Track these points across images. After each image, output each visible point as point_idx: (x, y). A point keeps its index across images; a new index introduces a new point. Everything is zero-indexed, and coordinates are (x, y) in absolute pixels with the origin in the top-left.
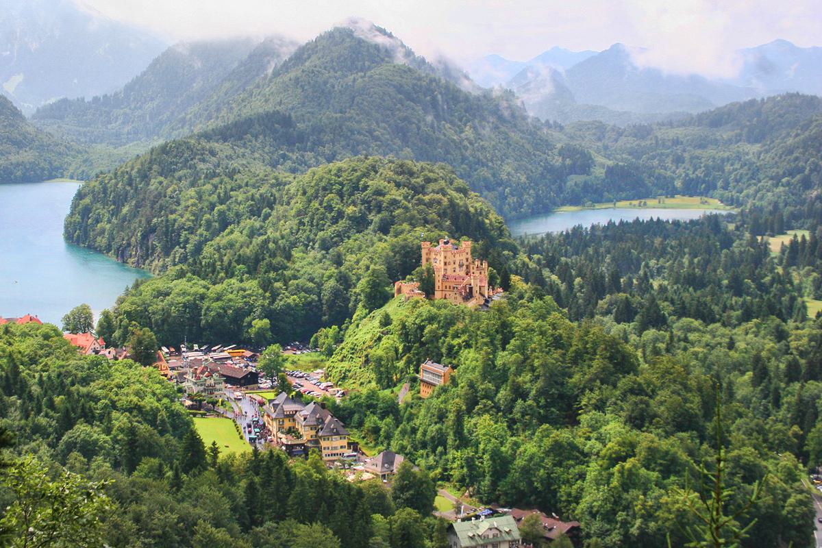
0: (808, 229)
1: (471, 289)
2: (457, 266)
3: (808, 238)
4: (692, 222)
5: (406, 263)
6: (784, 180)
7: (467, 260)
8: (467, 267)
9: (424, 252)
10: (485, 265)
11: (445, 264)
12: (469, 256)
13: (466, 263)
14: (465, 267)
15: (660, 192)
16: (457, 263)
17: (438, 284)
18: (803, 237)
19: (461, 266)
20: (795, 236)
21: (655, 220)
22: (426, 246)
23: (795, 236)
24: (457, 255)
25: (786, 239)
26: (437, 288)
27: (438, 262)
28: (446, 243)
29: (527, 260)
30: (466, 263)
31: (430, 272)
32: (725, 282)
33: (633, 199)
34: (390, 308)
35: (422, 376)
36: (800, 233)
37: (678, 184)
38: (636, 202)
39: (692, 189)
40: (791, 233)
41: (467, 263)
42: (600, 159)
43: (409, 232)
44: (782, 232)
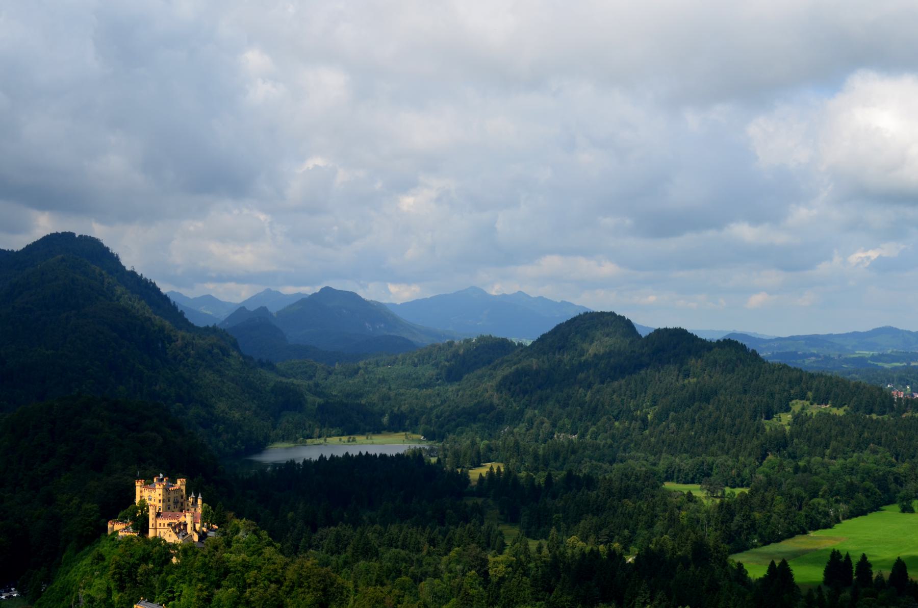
0: (502, 462)
1: (185, 525)
3: (502, 470)
4: (398, 455)
5: (122, 503)
6: (480, 416)
9: (138, 489)
15: (368, 428)
16: (172, 500)
18: (499, 469)
20: (491, 468)
21: (364, 453)
22: (138, 485)
23: (491, 468)
24: (172, 493)
25: (484, 471)
26: (150, 526)
28: (162, 480)
32: (429, 513)
33: (342, 435)
34: (104, 547)
36: (495, 466)
37: (385, 420)
38: (345, 438)
39: (398, 424)
40: (489, 465)
42: (310, 398)
44: (477, 465)
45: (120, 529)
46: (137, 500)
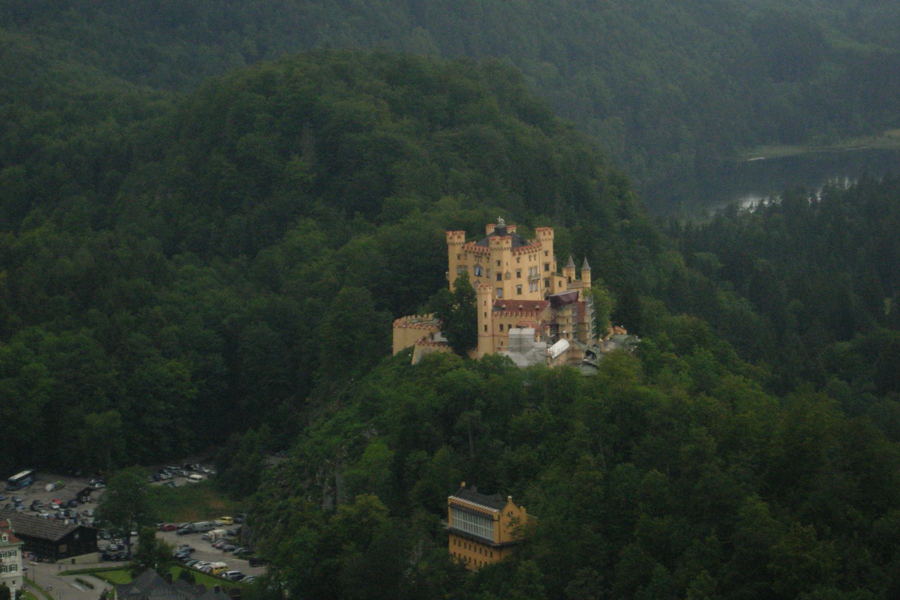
2: (524, 281)
7: (547, 267)
8: (547, 283)
9: (454, 252)
10: (587, 277)
11: (499, 277)
12: (551, 259)
13: (543, 274)
14: (542, 283)
16: (525, 274)
17: (482, 321)
19: (532, 281)
22: (456, 240)
26: (481, 330)
27: (484, 273)
29: (678, 260)
30: (543, 274)
31: (467, 295)
35: (456, 521)
41: (547, 274)
43: (424, 209)
45: (414, 336)
46: (452, 275)
